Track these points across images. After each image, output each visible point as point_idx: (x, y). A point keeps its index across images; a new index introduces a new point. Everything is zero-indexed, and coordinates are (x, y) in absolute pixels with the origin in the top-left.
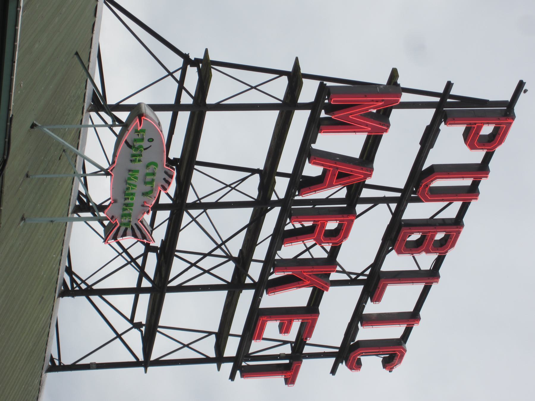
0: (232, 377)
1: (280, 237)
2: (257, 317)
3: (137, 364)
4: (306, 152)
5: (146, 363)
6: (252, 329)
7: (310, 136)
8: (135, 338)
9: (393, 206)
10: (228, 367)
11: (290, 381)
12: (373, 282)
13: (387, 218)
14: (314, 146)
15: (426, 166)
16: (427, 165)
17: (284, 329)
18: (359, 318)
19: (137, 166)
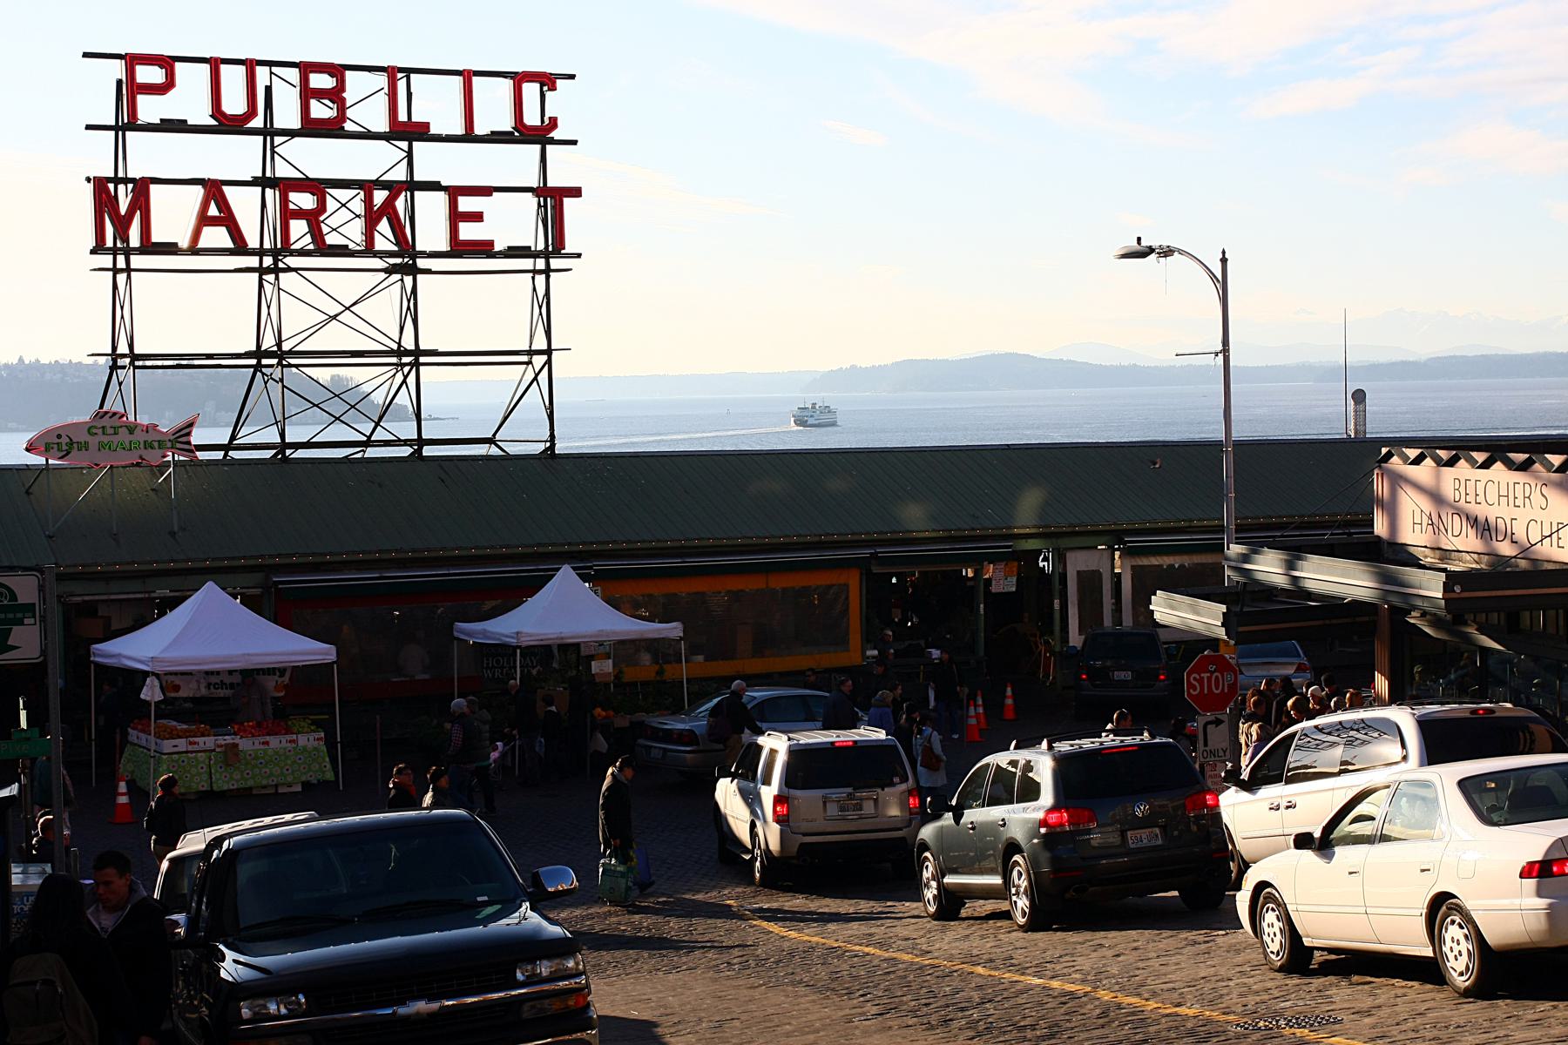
0: (579, 256)
1: (323, 249)
2: (459, 249)
3: (549, 362)
5: (548, 352)
6: (484, 249)
7: (170, 249)
8: (539, 360)
9: (278, 140)
10: (555, 263)
11: (576, 192)
12: (409, 132)
13: (298, 141)
14: (184, 243)
15: (214, 122)
16: (214, 122)
17: (477, 217)
18: (469, 137)
19: (93, 442)
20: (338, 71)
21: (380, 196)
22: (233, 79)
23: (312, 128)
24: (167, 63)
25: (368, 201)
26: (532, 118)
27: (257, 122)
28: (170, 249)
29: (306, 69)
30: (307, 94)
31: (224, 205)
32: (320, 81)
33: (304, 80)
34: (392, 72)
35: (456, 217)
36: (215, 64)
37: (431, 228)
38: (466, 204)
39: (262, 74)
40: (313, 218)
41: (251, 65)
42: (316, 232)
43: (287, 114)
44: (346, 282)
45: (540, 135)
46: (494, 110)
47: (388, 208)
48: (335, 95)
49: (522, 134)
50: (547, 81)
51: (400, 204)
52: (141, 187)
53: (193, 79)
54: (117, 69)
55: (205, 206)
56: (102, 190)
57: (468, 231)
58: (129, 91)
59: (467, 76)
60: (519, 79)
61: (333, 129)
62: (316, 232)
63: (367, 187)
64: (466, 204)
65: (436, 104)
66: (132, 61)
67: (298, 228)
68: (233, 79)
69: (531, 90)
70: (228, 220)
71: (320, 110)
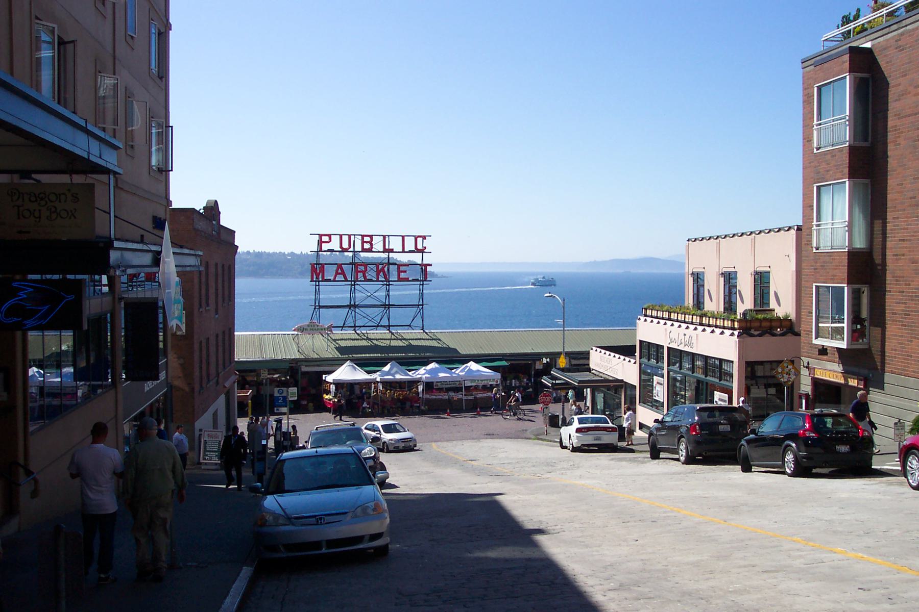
2: (400, 279)
4: (334, 281)
7: (329, 280)
18: (403, 251)
20: (371, 237)
21: (380, 267)
22: (345, 239)
23: (364, 250)
24: (330, 236)
25: (377, 268)
26: (420, 247)
27: (351, 249)
28: (329, 280)
29: (363, 236)
30: (363, 242)
31: (342, 269)
32: (367, 239)
33: (363, 239)
34: (384, 237)
35: (399, 272)
36: (341, 236)
37: (394, 276)
38: (402, 268)
39: (352, 237)
40: (364, 273)
41: (350, 236)
42: (365, 277)
43: (358, 248)
44: (371, 287)
45: (422, 251)
46: (410, 245)
47: (383, 269)
48: (371, 243)
49: (417, 251)
50: (424, 238)
51: (386, 269)
52: (323, 265)
53: (336, 239)
54: (317, 237)
55: (337, 271)
56: (313, 265)
57: (403, 275)
58: (320, 242)
59: (403, 237)
60: (416, 238)
61: (370, 250)
62: (365, 277)
63: (377, 265)
64: (402, 268)
65: (395, 244)
66: (321, 236)
67: (360, 275)
68: (345, 239)
69: (420, 240)
70: (343, 273)
71: (367, 246)
